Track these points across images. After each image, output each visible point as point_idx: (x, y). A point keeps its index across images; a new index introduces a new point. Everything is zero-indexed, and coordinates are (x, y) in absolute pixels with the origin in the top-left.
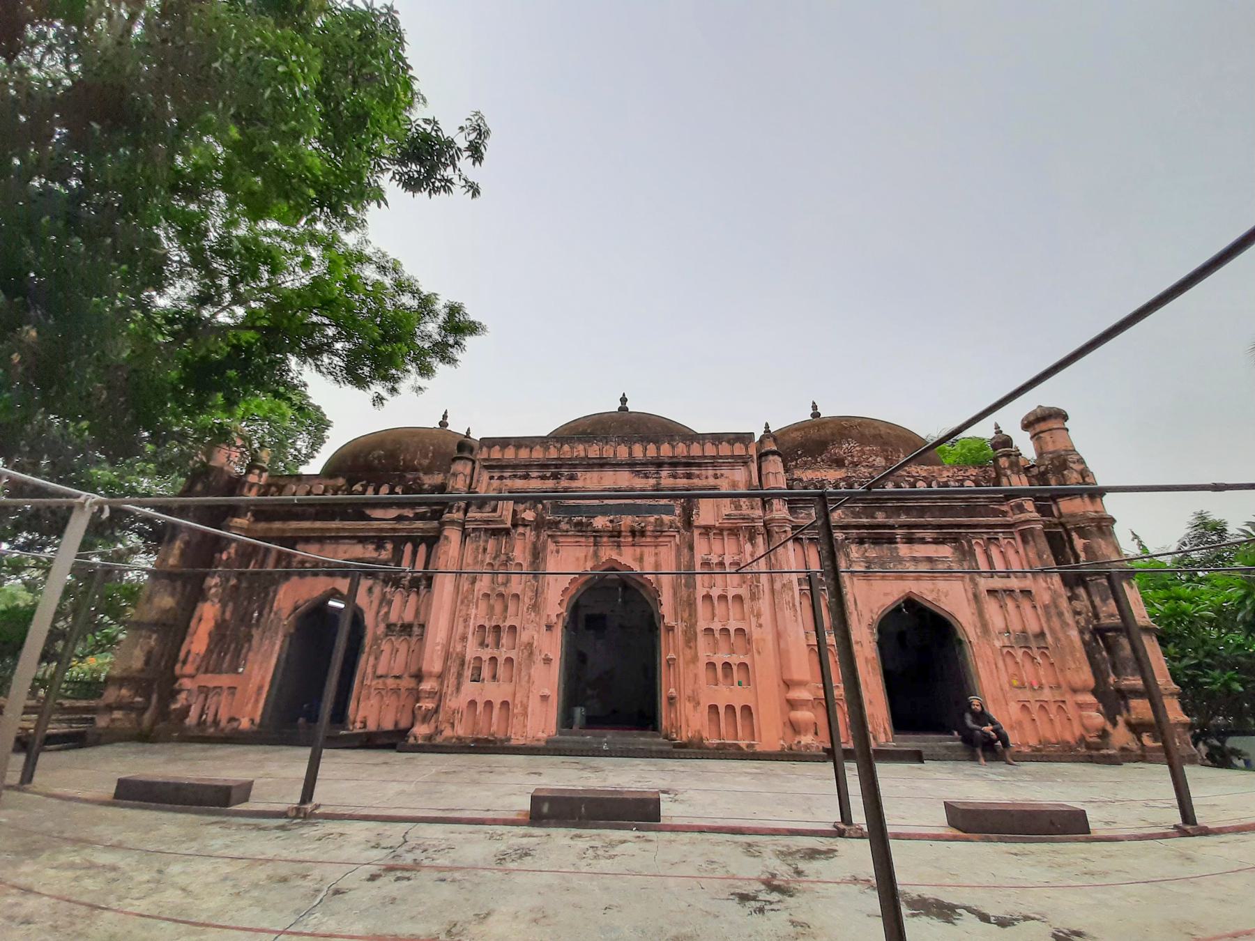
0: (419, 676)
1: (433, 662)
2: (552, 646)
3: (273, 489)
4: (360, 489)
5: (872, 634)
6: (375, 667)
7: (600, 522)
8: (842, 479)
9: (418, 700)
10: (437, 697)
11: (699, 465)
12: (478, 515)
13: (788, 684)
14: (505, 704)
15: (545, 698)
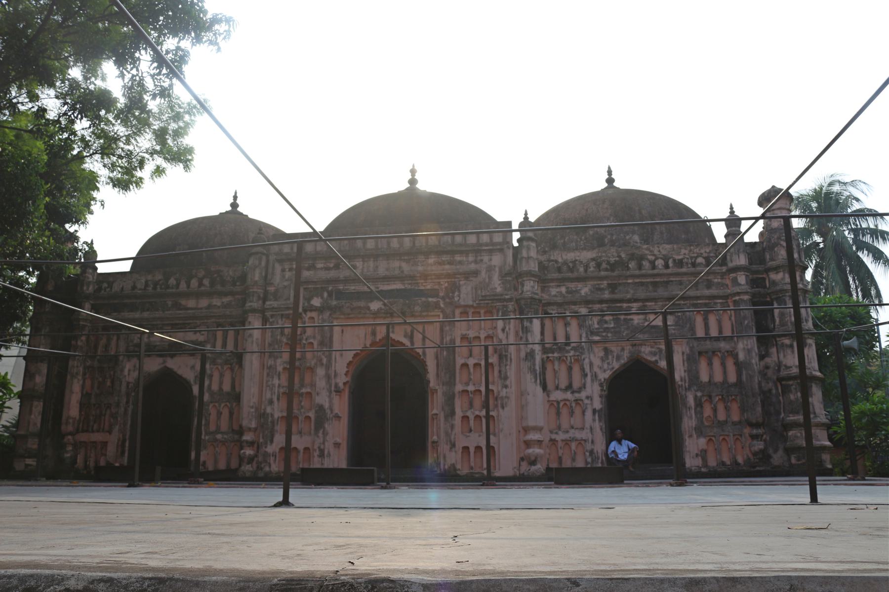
0: (241, 432)
1: (249, 421)
2: (341, 406)
3: (105, 285)
4: (175, 282)
5: (602, 390)
6: (207, 424)
7: (375, 306)
8: (593, 259)
9: (242, 448)
10: (256, 445)
11: (461, 252)
12: (275, 304)
13: (526, 430)
14: (306, 449)
15: (337, 445)
